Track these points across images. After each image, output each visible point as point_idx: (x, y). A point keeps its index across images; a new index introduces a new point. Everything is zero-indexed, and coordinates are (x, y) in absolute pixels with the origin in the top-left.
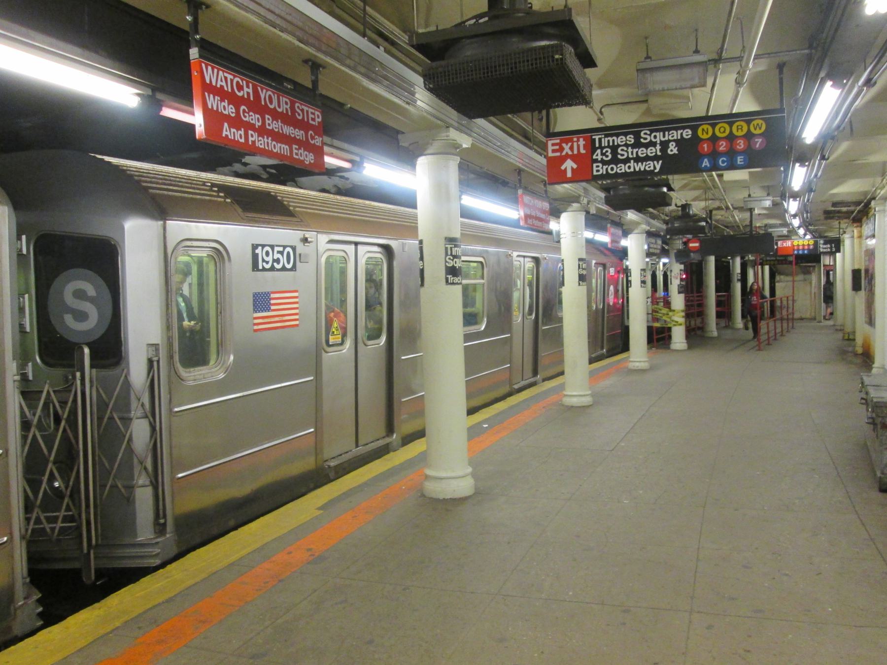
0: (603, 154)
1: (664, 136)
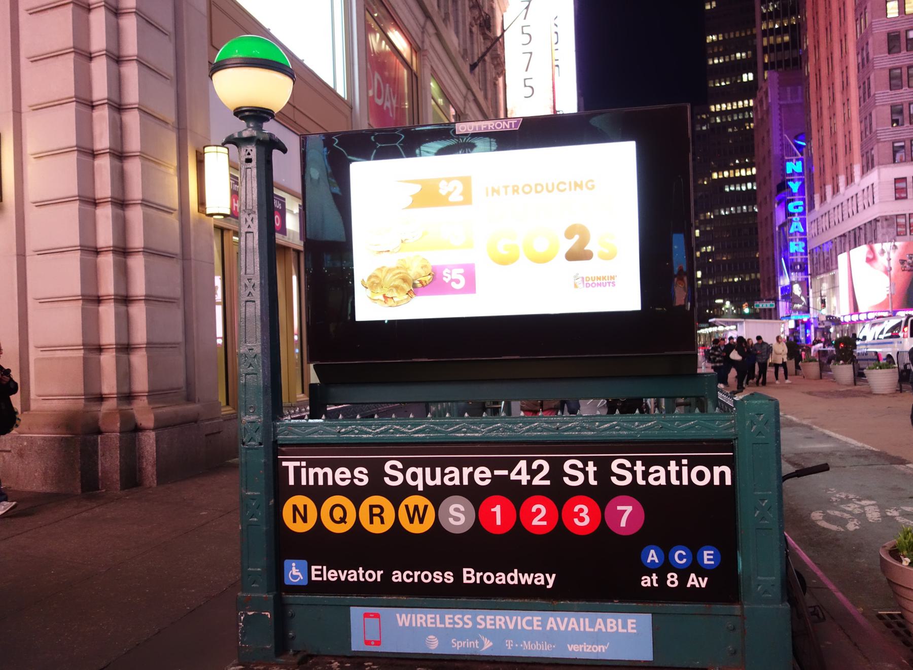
1: (433, 478)
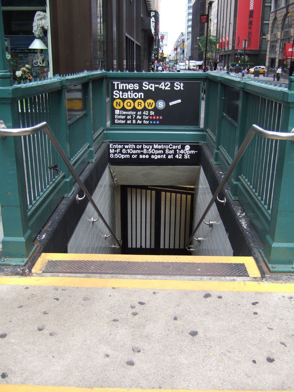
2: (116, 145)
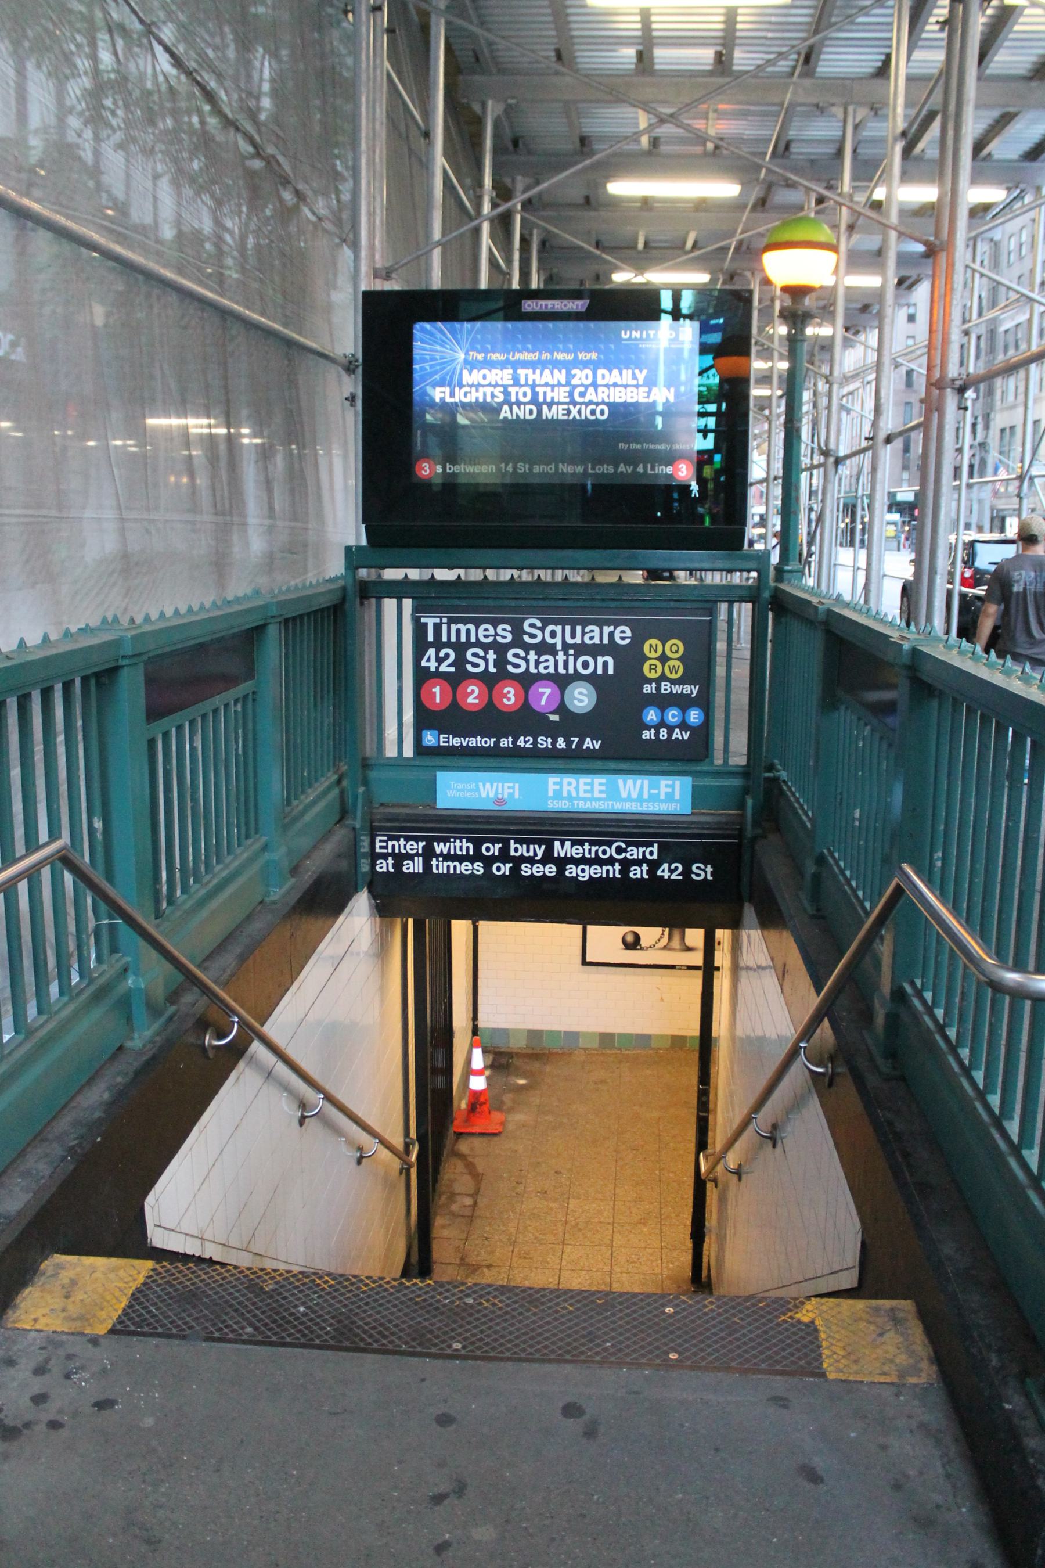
0: (440, 660)
2: (397, 839)
